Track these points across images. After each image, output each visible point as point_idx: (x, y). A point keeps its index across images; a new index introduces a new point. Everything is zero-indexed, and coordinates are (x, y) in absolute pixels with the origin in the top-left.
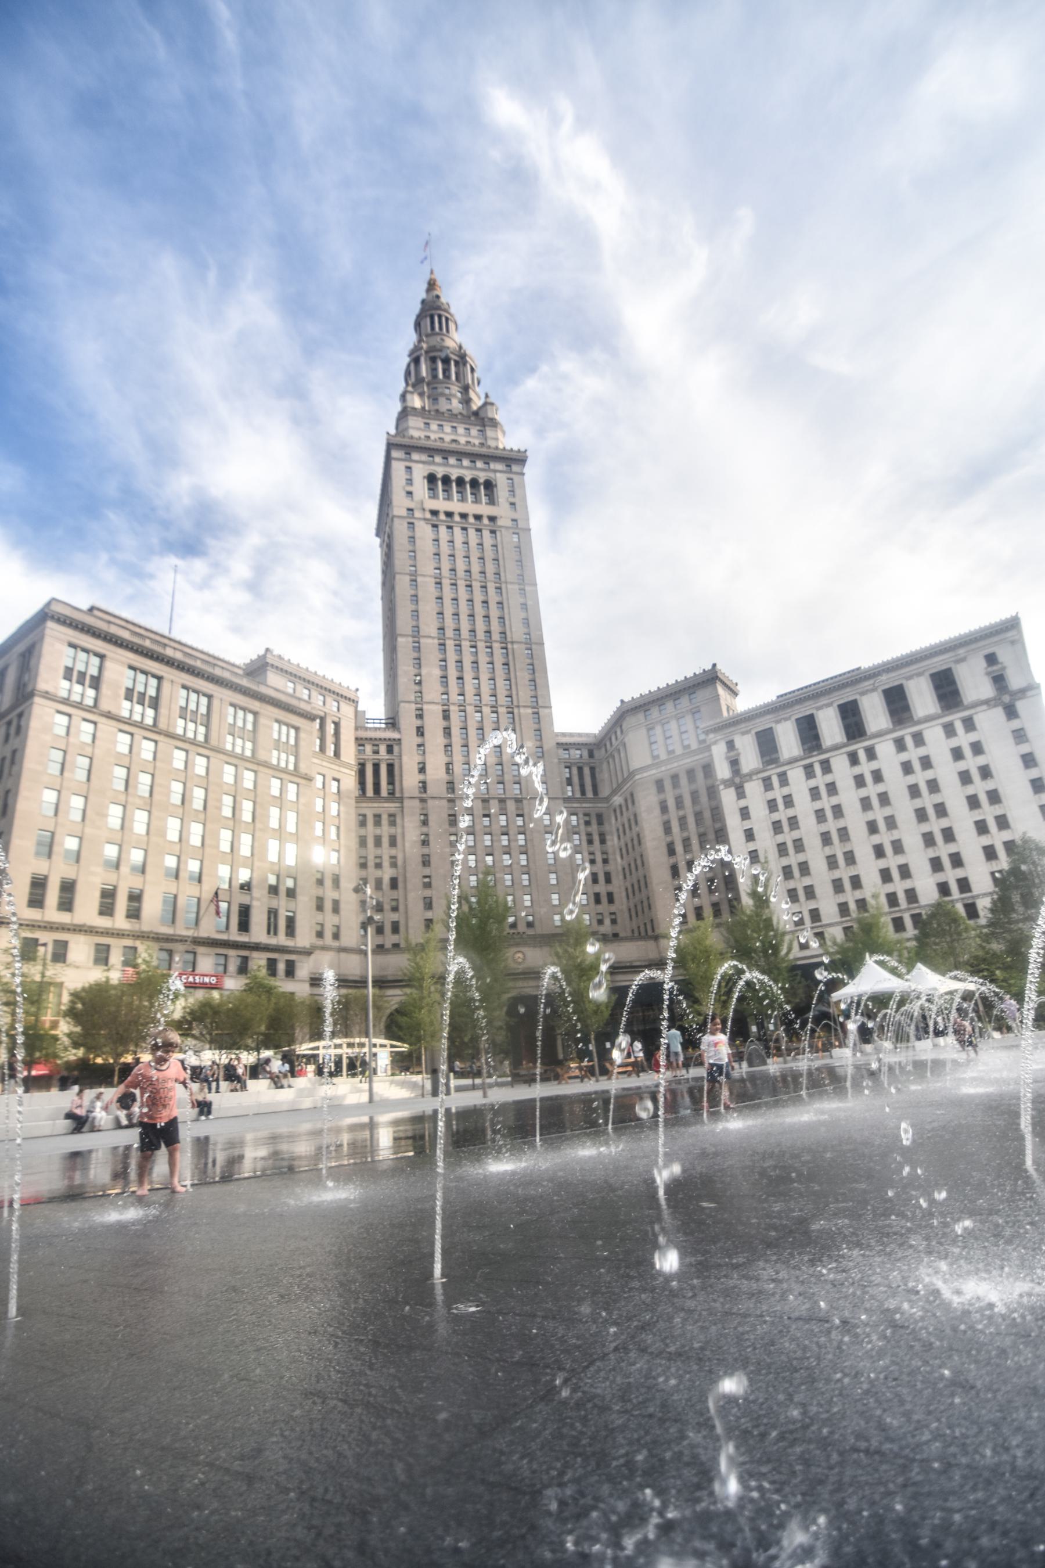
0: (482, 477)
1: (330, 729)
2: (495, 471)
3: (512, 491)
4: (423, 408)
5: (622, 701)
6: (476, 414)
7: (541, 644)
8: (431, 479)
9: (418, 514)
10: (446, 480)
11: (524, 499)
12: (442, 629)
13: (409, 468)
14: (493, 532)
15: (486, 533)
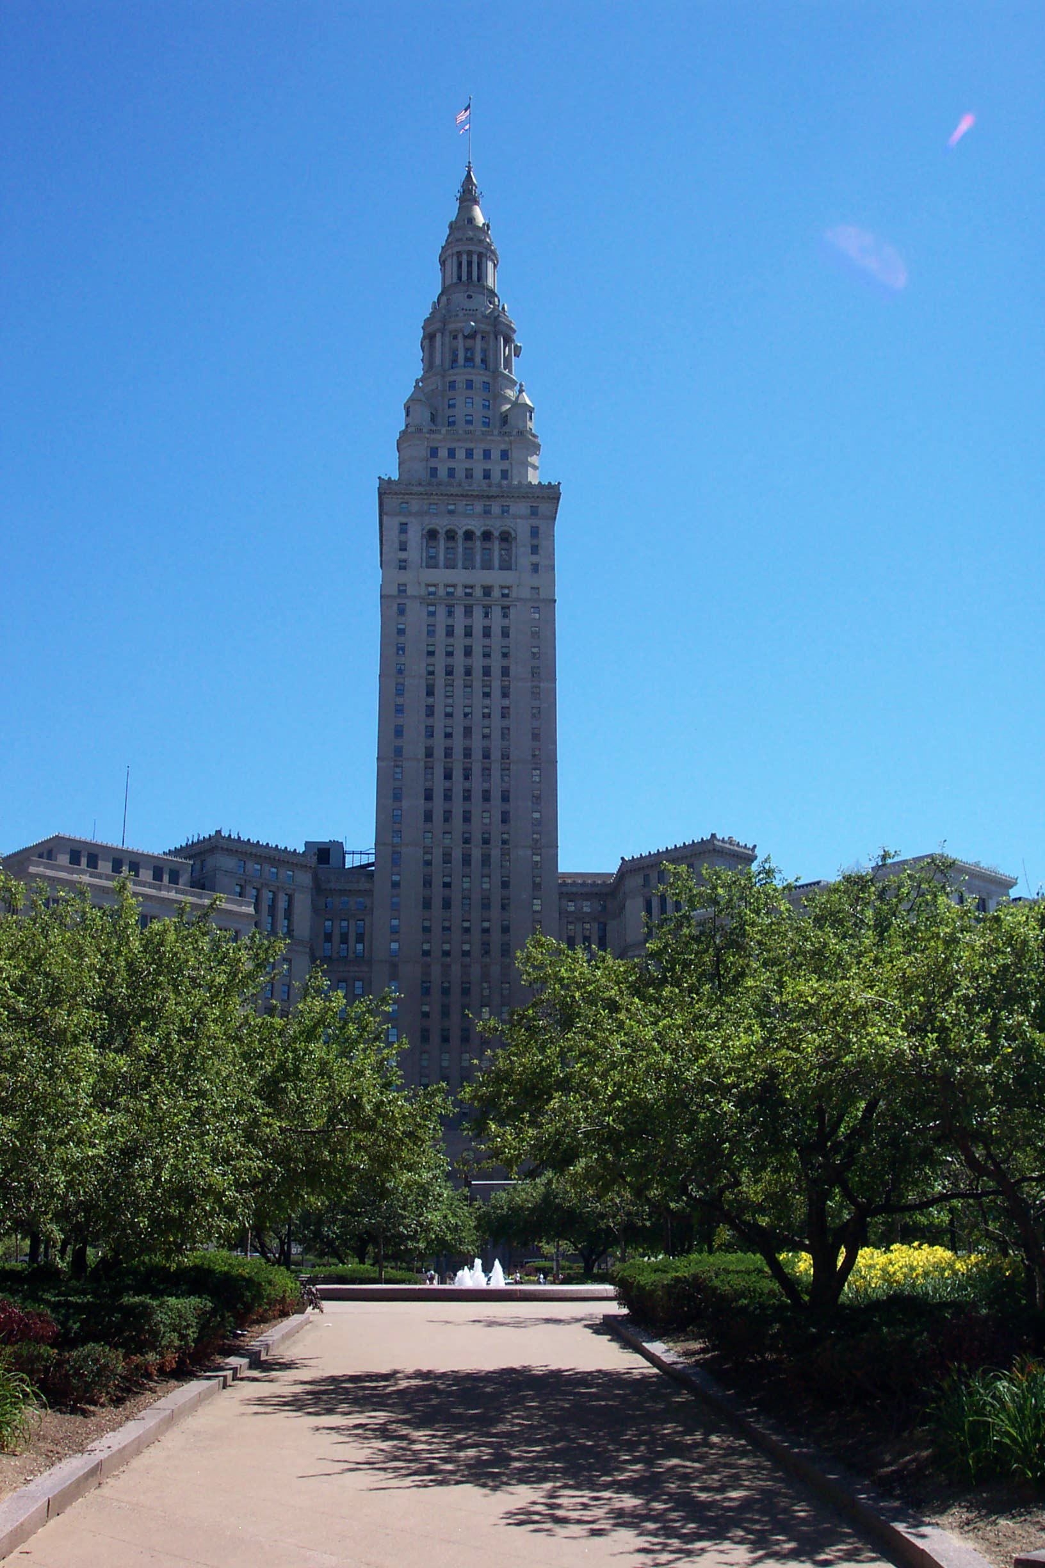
0: (496, 526)
1: (282, 904)
2: (515, 517)
3: (535, 550)
4: (433, 419)
5: (623, 859)
6: (505, 419)
7: (554, 762)
8: (432, 535)
9: (410, 591)
10: (451, 536)
11: (551, 556)
12: (429, 753)
13: (403, 528)
14: (505, 609)
15: (497, 612)
